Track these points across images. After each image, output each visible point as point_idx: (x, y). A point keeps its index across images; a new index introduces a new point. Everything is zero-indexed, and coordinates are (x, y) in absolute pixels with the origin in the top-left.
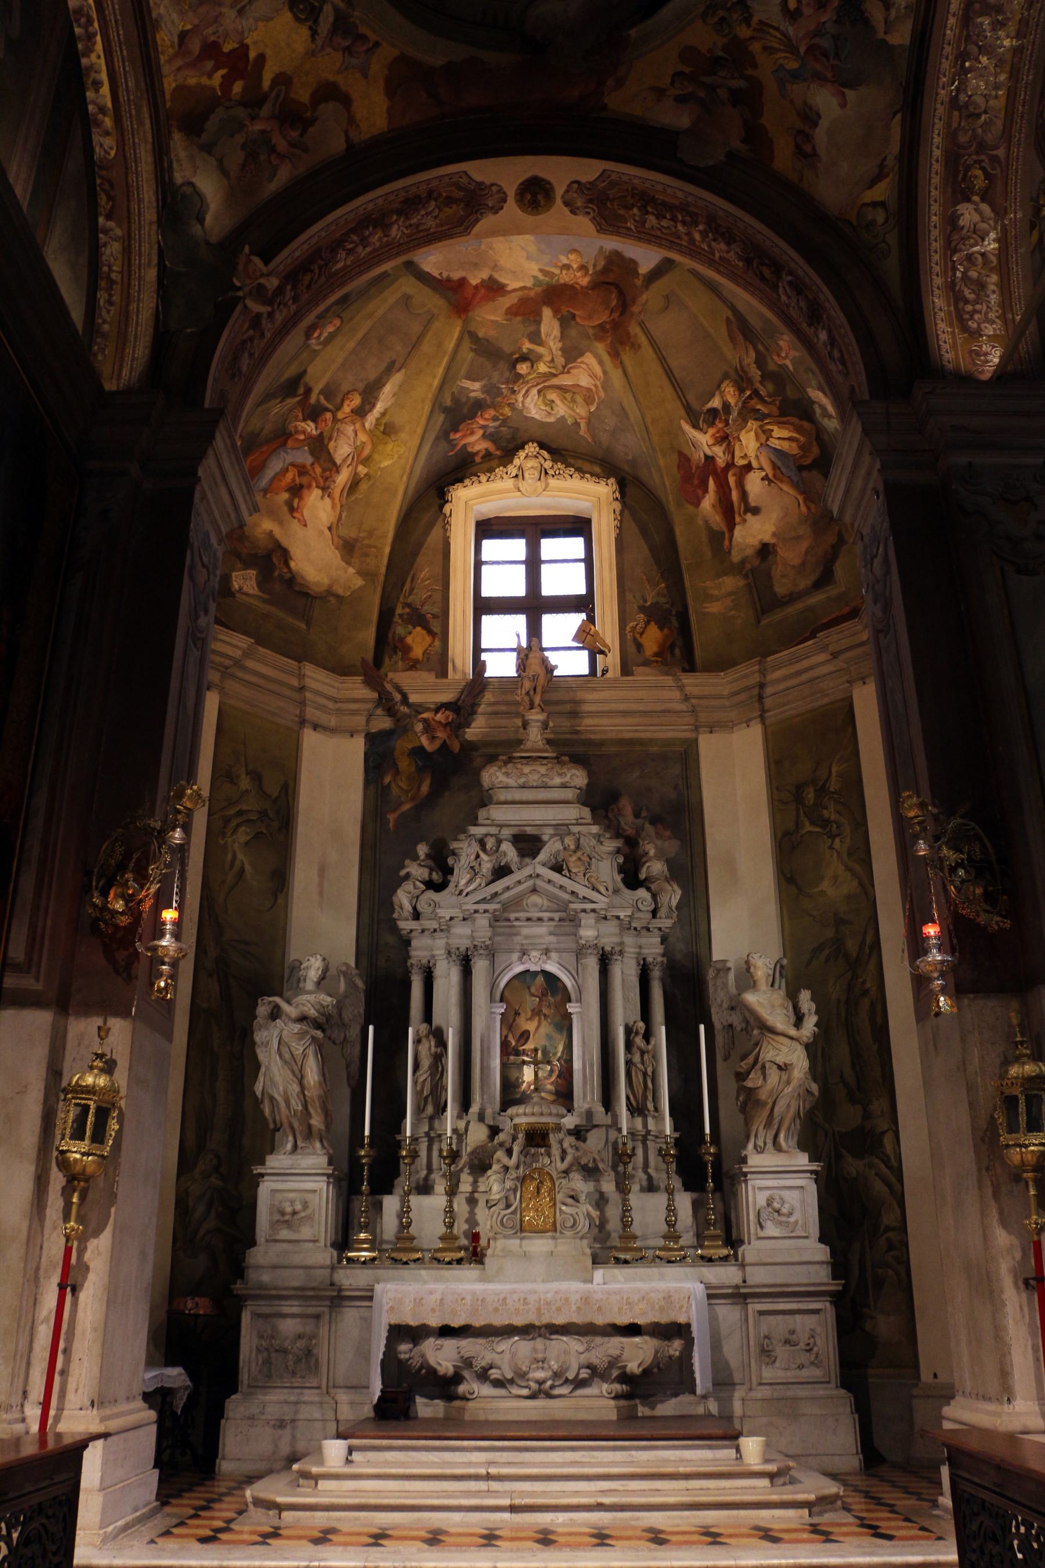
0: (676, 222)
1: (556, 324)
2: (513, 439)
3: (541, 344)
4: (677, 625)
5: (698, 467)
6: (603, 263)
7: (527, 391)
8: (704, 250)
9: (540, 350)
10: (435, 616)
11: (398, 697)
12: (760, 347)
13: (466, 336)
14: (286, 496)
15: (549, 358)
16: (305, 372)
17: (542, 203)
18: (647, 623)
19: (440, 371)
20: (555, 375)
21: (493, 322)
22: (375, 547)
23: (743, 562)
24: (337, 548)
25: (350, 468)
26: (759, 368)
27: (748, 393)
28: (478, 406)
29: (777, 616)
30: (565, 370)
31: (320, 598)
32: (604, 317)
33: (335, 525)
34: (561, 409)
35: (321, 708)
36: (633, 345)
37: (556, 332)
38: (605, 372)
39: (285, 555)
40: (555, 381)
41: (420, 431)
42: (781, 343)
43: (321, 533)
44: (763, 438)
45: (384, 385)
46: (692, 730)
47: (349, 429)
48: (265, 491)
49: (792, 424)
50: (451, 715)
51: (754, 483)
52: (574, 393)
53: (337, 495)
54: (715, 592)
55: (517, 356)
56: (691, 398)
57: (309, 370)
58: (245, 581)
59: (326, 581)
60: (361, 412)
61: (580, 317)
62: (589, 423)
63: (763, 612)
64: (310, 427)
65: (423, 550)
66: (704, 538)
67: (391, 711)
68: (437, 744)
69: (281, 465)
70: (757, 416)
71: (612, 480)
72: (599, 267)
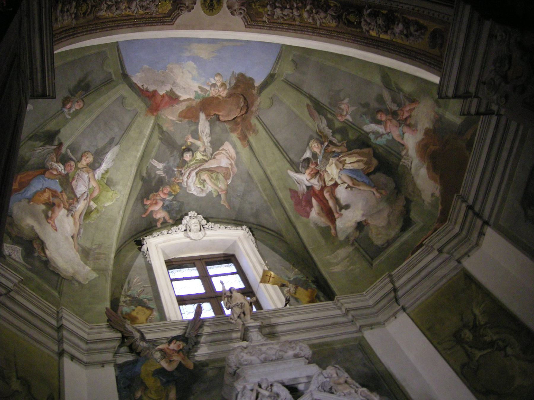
0: (292, 9)
1: (207, 124)
2: (180, 211)
3: (198, 138)
4: (315, 287)
5: (303, 195)
6: (234, 82)
7: (189, 174)
8: (310, 23)
9: (198, 143)
10: (149, 300)
11: (137, 335)
12: (329, 116)
13: (157, 127)
14: (43, 207)
15: (202, 149)
17: (216, 6)
18: (296, 288)
19: (142, 148)
20: (206, 161)
21: (171, 120)
22: (104, 254)
23: (347, 238)
24: (78, 251)
25: (86, 201)
26: (330, 128)
27: (326, 144)
28: (161, 182)
29: (383, 256)
30: (213, 157)
31: (67, 280)
32: (236, 113)
33: (76, 236)
34: (210, 187)
35: (75, 346)
36: (254, 131)
37: (207, 130)
38: (237, 153)
39: (43, 245)
40: (206, 166)
41: (130, 184)
42: (343, 106)
43: (67, 238)
44: (341, 166)
45: (107, 153)
46: (357, 332)
47: (86, 176)
48: (30, 200)
49: (357, 153)
50: (182, 345)
51: (342, 193)
52: (218, 173)
53: (77, 216)
54: (335, 261)
55: (184, 147)
56: (292, 156)
57: (62, 131)
59: (71, 271)
60: (93, 167)
61: (222, 115)
62: (227, 193)
63: (372, 259)
64: (60, 167)
65: (133, 269)
66: (318, 234)
67: (132, 349)
68: (174, 366)
69: (40, 187)
70: (334, 155)
71: (244, 227)
72: (232, 85)
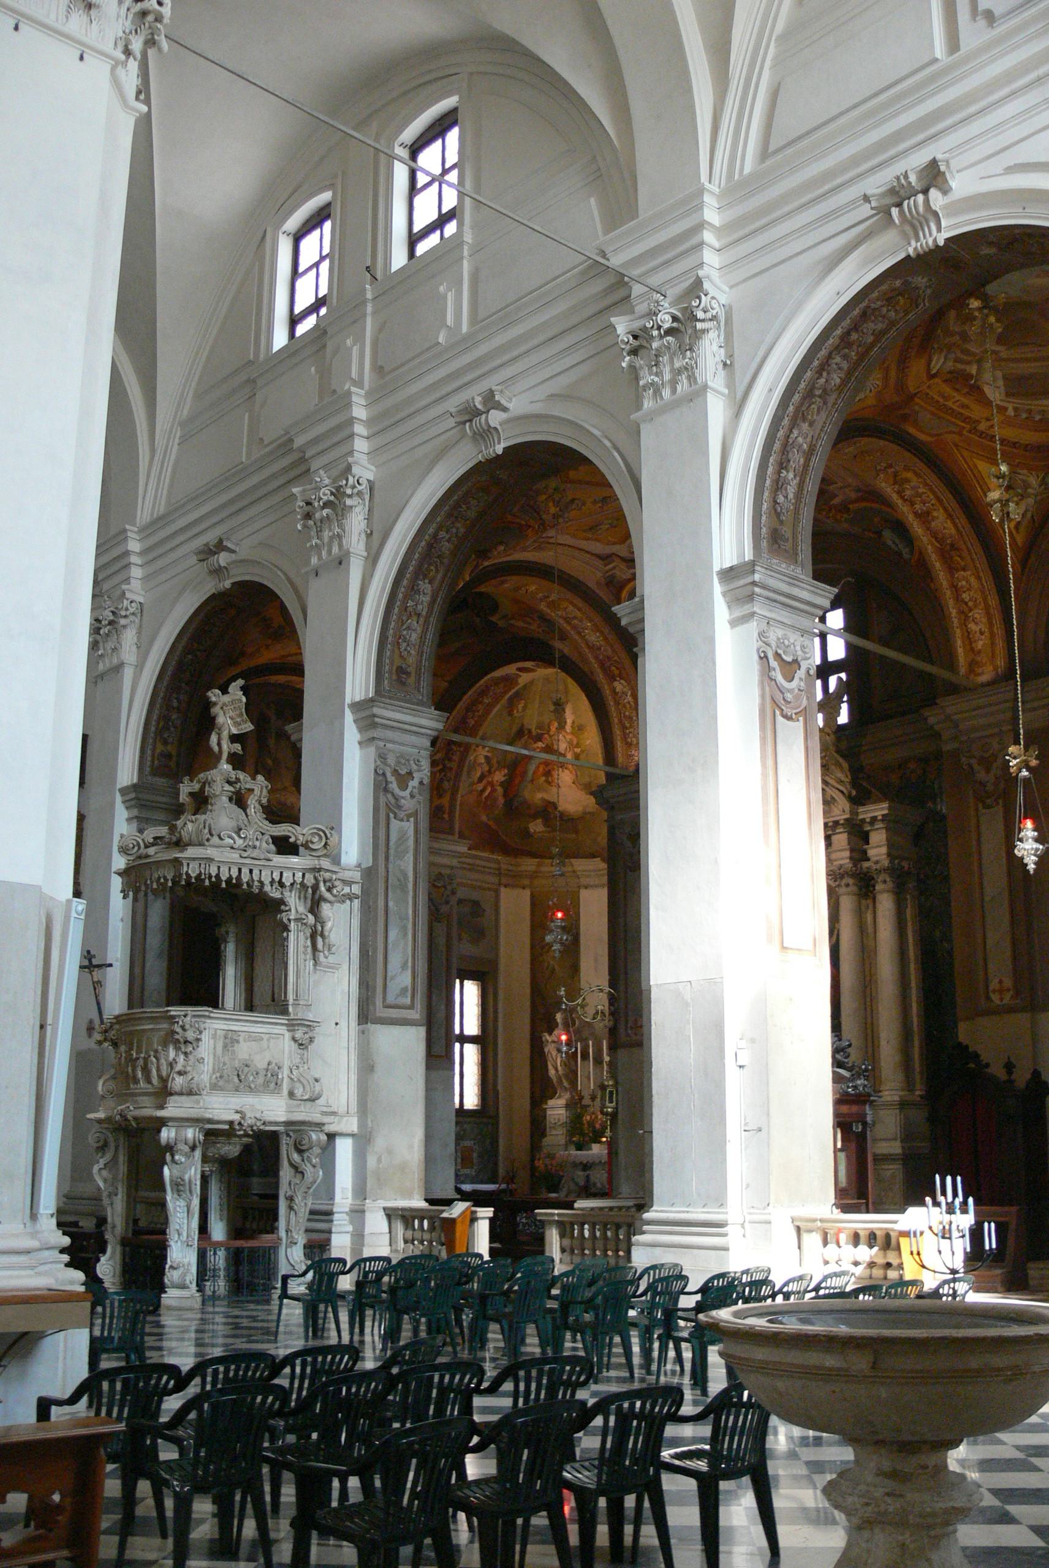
14: (543, 778)
16: (523, 725)
39: (554, 806)
48: (532, 781)
58: (537, 827)
59: (581, 809)
60: (562, 726)
64: (540, 744)
